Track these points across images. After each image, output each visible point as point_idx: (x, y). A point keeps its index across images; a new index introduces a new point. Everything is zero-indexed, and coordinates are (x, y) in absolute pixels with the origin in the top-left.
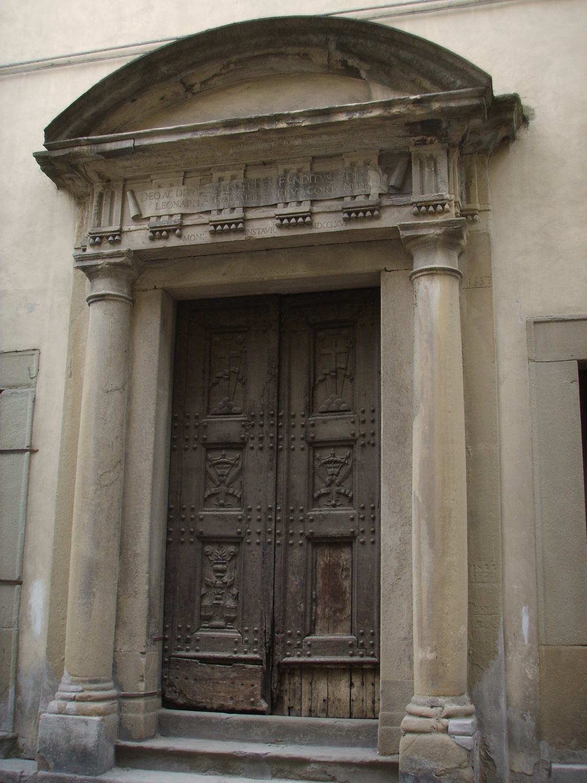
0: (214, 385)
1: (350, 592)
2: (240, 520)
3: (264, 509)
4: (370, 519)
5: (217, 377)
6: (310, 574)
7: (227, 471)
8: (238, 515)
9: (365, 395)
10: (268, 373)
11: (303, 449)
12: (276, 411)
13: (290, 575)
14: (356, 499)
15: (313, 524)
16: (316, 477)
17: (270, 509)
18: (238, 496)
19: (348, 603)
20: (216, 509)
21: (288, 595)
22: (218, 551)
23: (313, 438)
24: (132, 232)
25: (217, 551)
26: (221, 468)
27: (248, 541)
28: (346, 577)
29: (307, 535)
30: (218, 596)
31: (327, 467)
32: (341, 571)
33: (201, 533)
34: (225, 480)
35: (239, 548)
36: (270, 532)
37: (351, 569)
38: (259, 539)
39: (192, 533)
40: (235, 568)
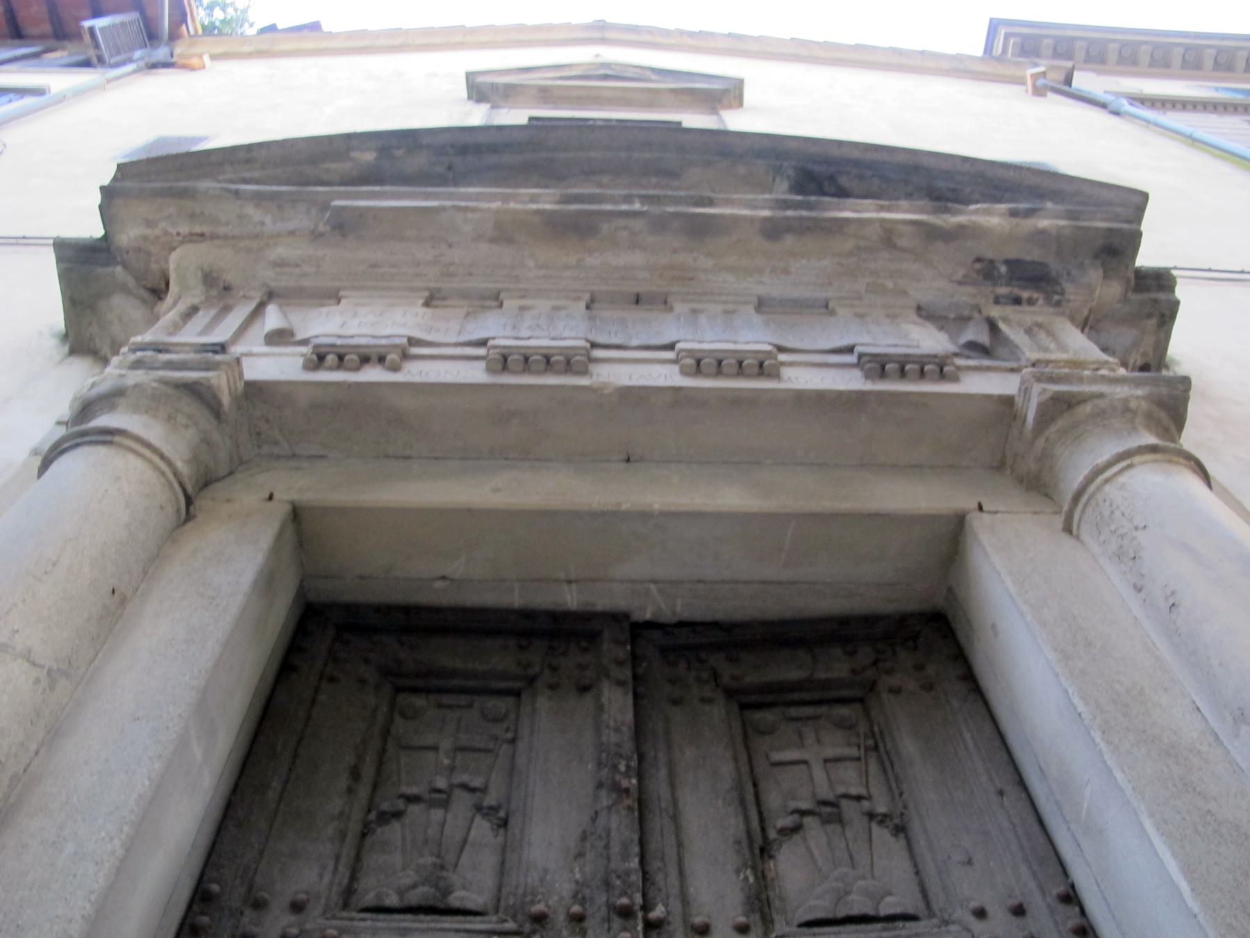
0: (387, 817)
5: (402, 796)
9: (970, 862)
10: (600, 785)
12: (638, 899)
24: (254, 358)
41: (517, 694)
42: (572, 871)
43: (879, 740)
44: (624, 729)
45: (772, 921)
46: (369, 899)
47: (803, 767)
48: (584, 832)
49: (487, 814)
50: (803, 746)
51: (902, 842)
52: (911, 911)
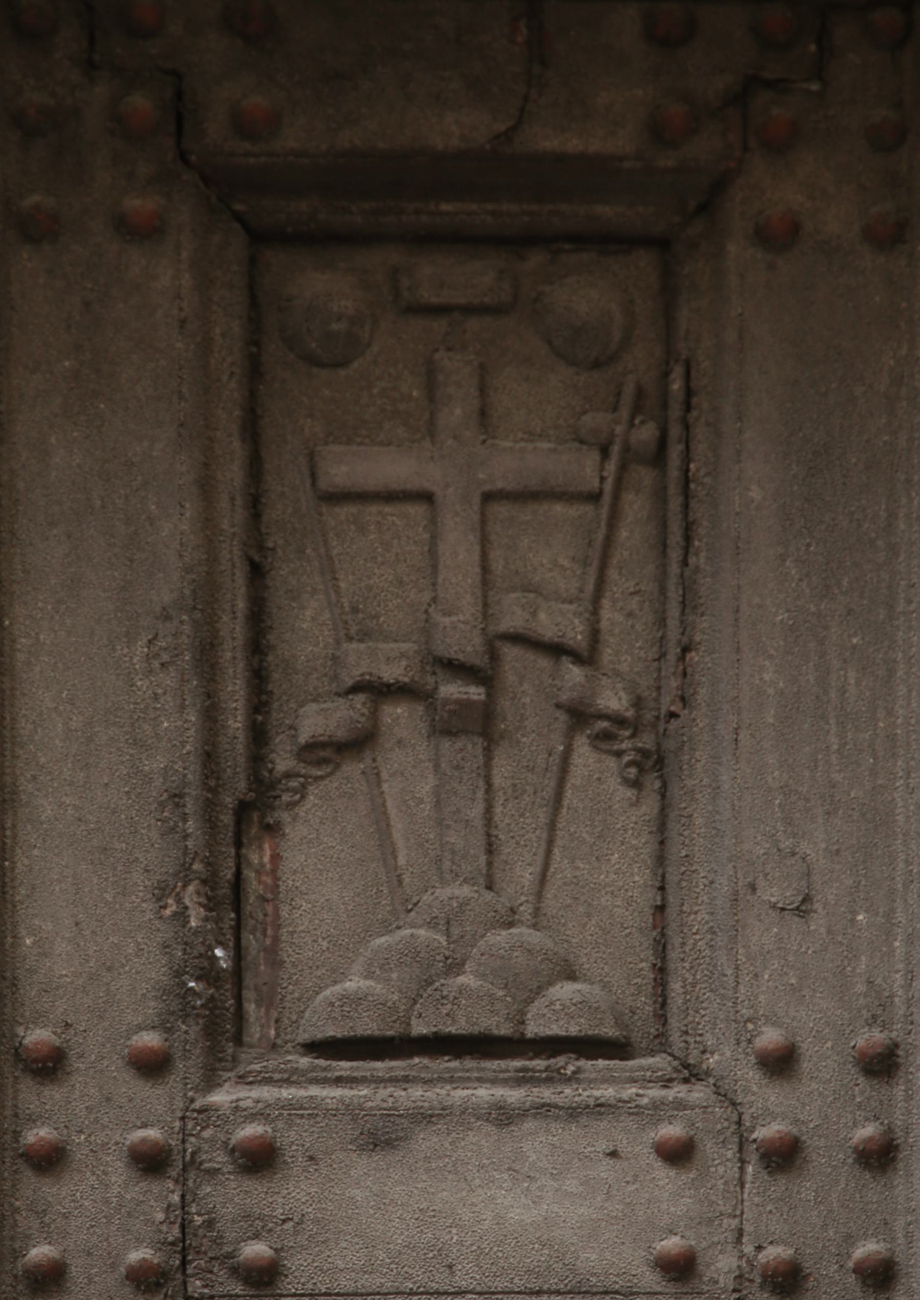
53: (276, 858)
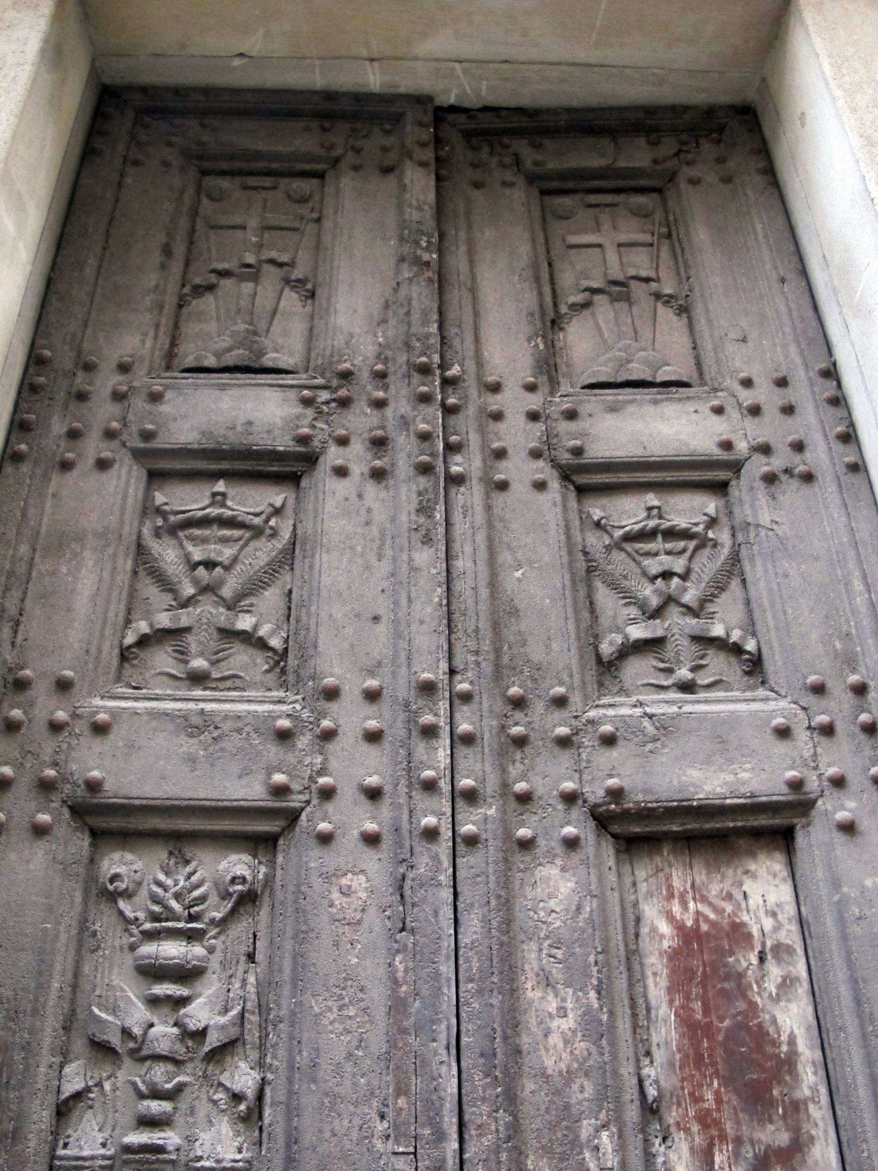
0: (200, 290)
1: (818, 1053)
2: (284, 736)
3: (403, 690)
4: (857, 730)
5: (213, 271)
6: (621, 983)
7: (227, 553)
8: (272, 717)
9: (744, 340)
10: (402, 259)
11: (540, 486)
12: (436, 358)
13: (529, 985)
14: (773, 664)
15: (614, 754)
16: (598, 584)
17: (428, 688)
18: (275, 642)
19: (819, 1113)
20: (169, 692)
21: (529, 1086)
22: (167, 874)
23: (578, 452)
25: (162, 877)
26: (205, 541)
27: (324, 826)
28: (787, 984)
29: (592, 799)
30: (156, 1107)
31: (637, 552)
32: (755, 961)
33: (93, 786)
34: (221, 583)
35: (272, 863)
36: (430, 786)
37: (800, 951)
38: (373, 818)
39: (46, 787)
40: (251, 957)
41: (320, 176)
42: (376, 336)
43: (673, 228)
44: (426, 207)
45: (558, 383)
46: (190, 361)
47: (597, 250)
48: (387, 302)
49: (295, 287)
50: (599, 231)
51: (685, 321)
52: (685, 379)
53: (564, 337)
